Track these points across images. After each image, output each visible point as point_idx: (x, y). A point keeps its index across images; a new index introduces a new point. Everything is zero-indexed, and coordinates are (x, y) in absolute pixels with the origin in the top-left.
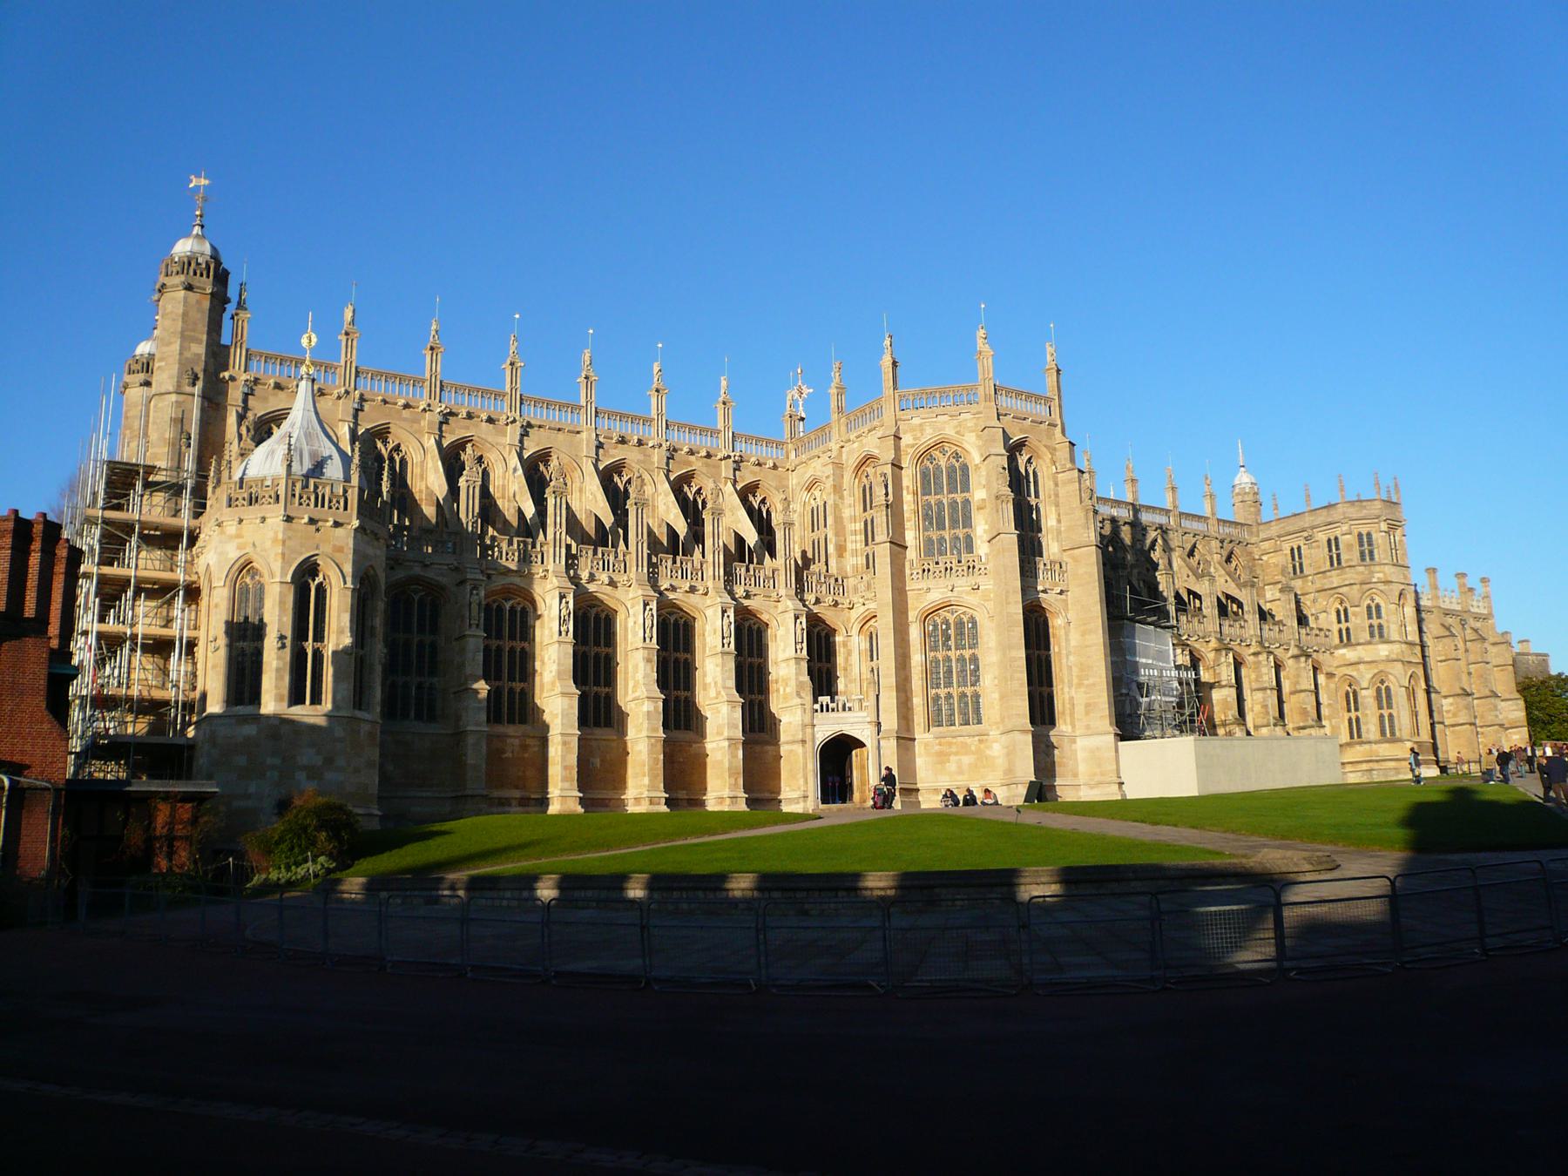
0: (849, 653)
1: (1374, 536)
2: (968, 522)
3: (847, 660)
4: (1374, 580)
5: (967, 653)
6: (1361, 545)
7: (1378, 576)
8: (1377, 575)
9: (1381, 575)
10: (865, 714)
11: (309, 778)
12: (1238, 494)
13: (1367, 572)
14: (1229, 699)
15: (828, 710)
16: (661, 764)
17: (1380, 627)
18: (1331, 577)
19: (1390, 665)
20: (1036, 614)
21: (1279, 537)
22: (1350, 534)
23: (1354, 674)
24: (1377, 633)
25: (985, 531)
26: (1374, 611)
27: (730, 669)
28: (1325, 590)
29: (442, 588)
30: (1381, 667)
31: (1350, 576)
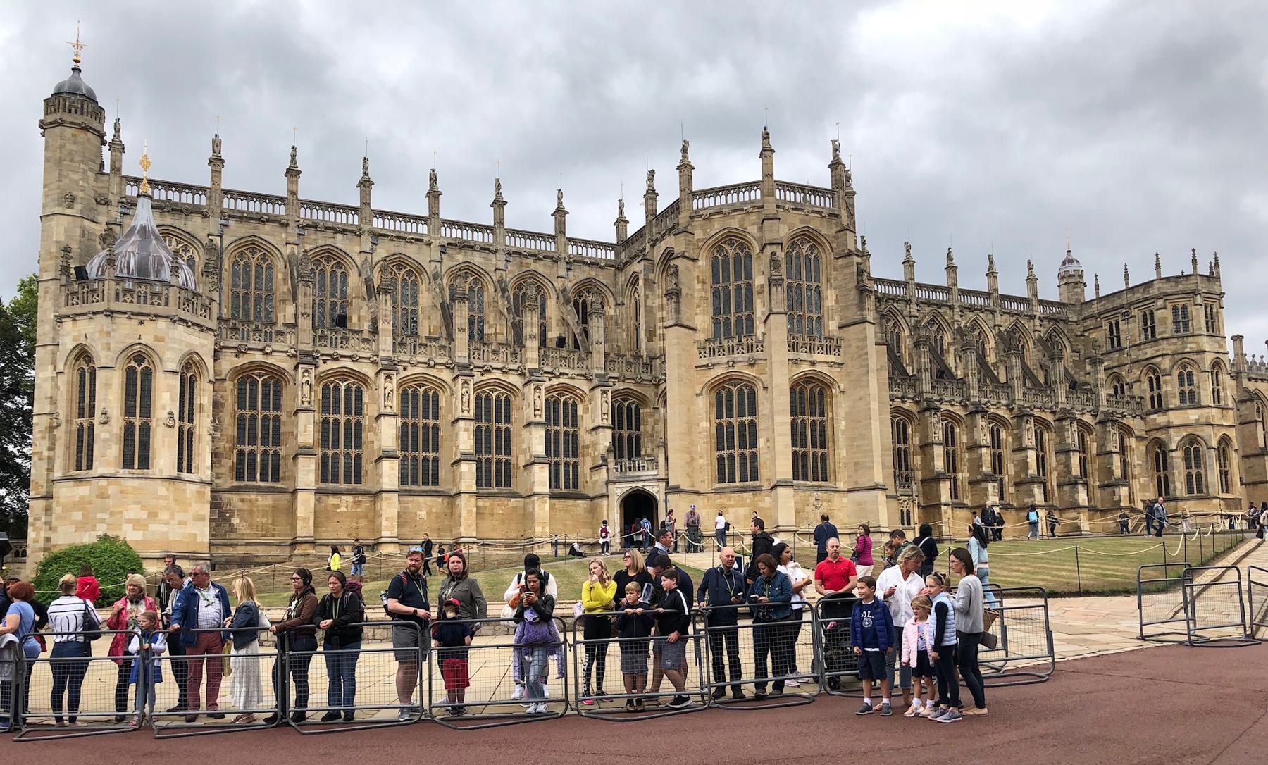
1: (1189, 309)
4: (1188, 350)
5: (747, 419)
6: (1175, 316)
7: (1191, 346)
8: (1189, 345)
9: (1194, 345)
11: (134, 529)
12: (1063, 277)
13: (1180, 343)
14: (1029, 460)
16: (474, 515)
17: (1191, 392)
20: (811, 385)
21: (1100, 314)
22: (1165, 308)
23: (1163, 437)
24: (1190, 400)
25: (763, 313)
26: (1186, 378)
27: (540, 437)
29: (281, 371)
30: (1191, 430)
31: (1166, 347)
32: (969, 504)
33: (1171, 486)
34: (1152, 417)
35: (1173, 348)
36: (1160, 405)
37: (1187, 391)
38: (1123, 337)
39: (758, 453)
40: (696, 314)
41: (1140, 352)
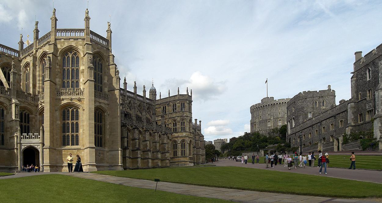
0: (36, 121)
2: (78, 77)
3: (35, 123)
4: (184, 116)
5: (75, 122)
8: (185, 114)
10: (38, 140)
14: (148, 144)
15: (26, 138)
17: (184, 127)
18: (173, 114)
19: (186, 138)
20: (98, 111)
23: (176, 140)
24: (183, 129)
25: (83, 80)
26: (183, 124)
28: (171, 118)
30: (183, 138)
31: (178, 114)
32: (131, 157)
33: (178, 154)
34: (174, 134)
35: (181, 115)
36: (176, 131)
37: (183, 127)
38: (167, 111)
39: (79, 135)
40: (56, 78)
41: (172, 115)
